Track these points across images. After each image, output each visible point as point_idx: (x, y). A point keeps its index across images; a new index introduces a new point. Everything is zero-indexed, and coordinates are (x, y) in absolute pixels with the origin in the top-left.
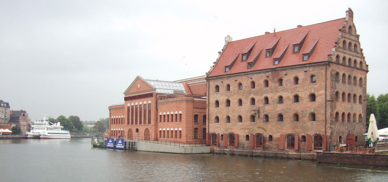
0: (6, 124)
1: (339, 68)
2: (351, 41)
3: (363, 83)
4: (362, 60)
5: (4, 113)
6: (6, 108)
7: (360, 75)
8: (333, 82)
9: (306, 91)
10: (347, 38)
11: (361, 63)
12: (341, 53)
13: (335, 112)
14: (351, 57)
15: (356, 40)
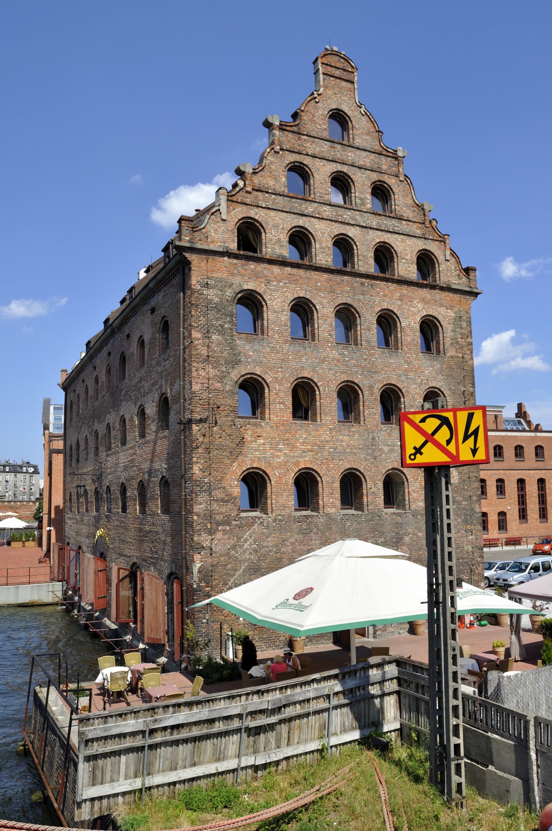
0: (31, 504)
1: (256, 276)
2: (345, 169)
3: (448, 342)
4: (434, 247)
5: (27, 483)
6: (32, 475)
7: (420, 306)
8: (214, 337)
9: (154, 389)
10: (314, 157)
11: (425, 261)
12: (272, 213)
13: (237, 469)
14: (351, 232)
15: (384, 167)
